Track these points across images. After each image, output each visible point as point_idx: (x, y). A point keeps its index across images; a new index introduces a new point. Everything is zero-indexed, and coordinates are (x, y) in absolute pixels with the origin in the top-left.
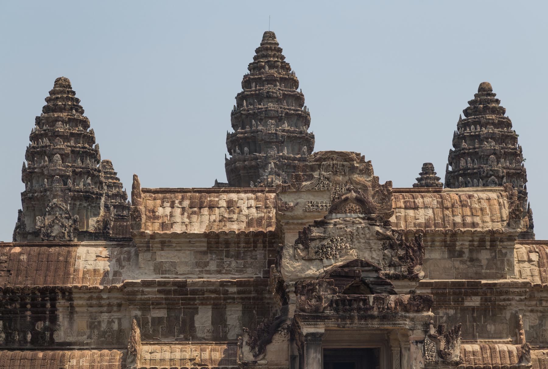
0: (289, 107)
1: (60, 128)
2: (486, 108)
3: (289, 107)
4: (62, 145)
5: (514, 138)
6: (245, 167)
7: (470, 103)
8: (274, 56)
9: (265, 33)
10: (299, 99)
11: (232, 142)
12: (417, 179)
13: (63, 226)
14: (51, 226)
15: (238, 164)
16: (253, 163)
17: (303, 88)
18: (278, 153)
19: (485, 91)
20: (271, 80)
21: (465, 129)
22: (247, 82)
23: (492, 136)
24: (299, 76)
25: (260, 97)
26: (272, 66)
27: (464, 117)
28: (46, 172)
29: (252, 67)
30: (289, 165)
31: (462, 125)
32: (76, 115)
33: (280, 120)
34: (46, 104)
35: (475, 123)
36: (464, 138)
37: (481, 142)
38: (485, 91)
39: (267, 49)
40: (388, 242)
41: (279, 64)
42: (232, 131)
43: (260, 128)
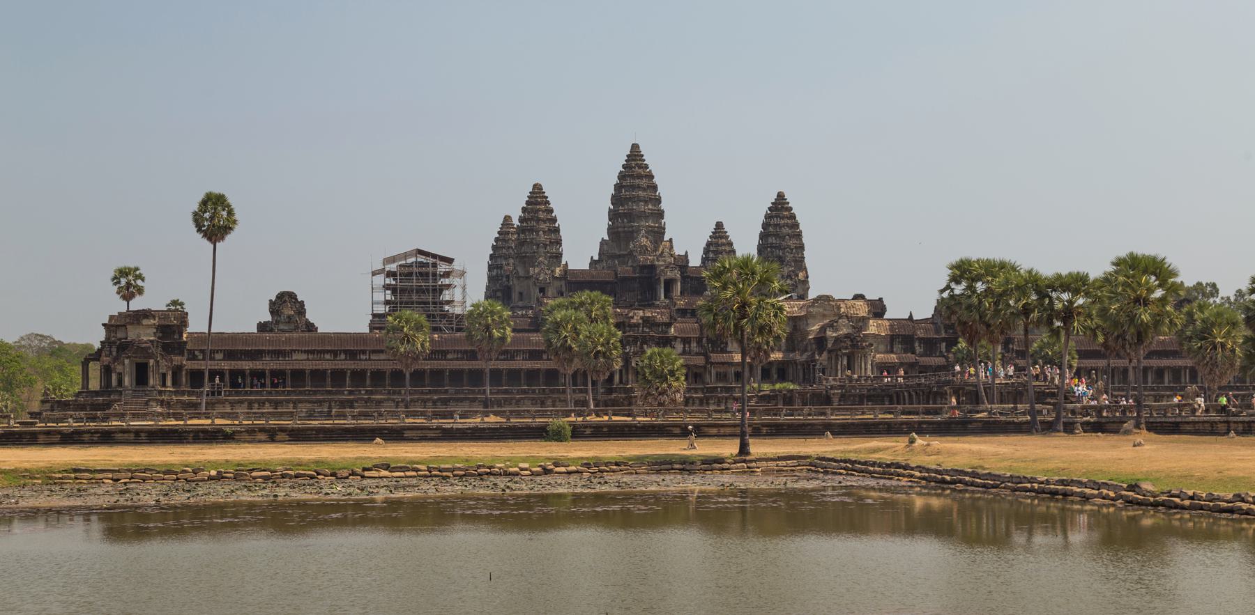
0: (650, 194)
1: (541, 215)
3: (650, 194)
4: (543, 226)
5: (797, 225)
10: (655, 188)
17: (657, 180)
19: (781, 196)
20: (640, 177)
22: (622, 176)
23: (787, 225)
25: (633, 187)
26: (640, 167)
31: (767, 216)
33: (646, 202)
35: (777, 217)
38: (781, 196)
40: (853, 327)
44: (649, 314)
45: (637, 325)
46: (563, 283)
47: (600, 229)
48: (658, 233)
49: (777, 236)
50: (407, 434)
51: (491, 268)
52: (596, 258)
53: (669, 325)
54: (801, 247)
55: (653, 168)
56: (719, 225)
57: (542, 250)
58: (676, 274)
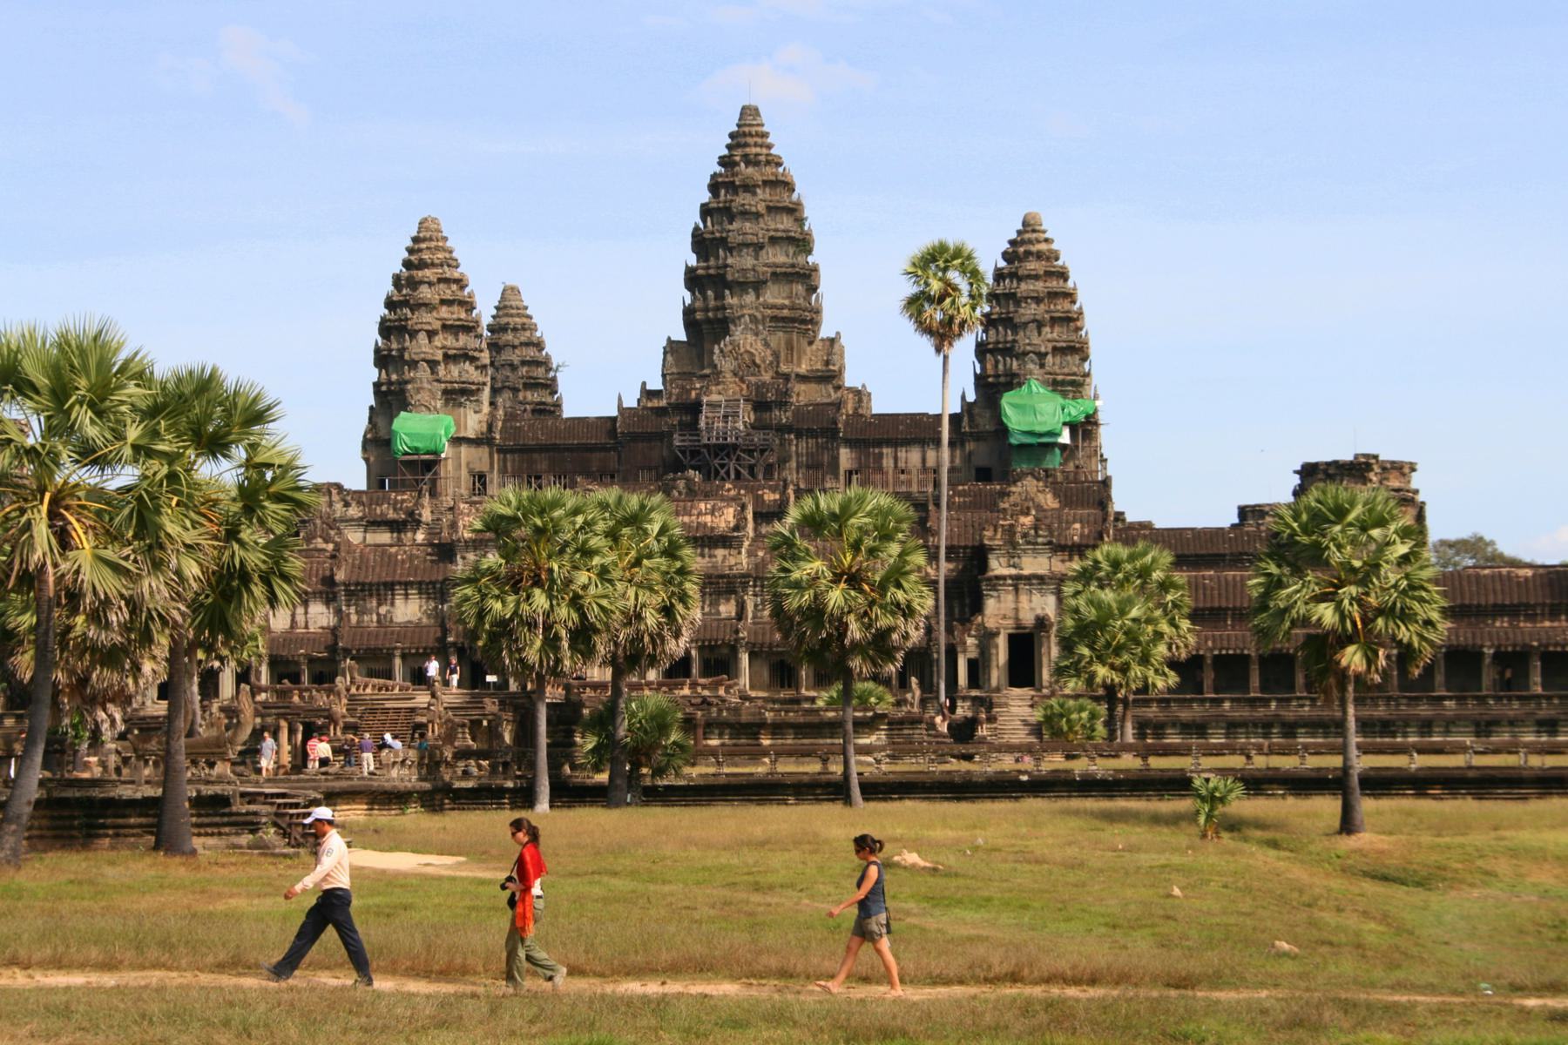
1: (425, 293)
2: (1028, 253)
6: (708, 321)
7: (1012, 243)
8: (756, 145)
9: (744, 108)
11: (693, 280)
16: (720, 315)
18: (758, 297)
20: (749, 188)
26: (750, 161)
27: (1002, 264)
28: (407, 357)
29: (724, 161)
30: (774, 319)
32: (448, 273)
34: (406, 254)
35: (1013, 275)
37: (1018, 303)
39: (744, 135)
41: (762, 158)
42: (692, 260)
43: (730, 261)
47: (664, 313)
48: (803, 321)
55: (794, 166)
57: (423, 372)
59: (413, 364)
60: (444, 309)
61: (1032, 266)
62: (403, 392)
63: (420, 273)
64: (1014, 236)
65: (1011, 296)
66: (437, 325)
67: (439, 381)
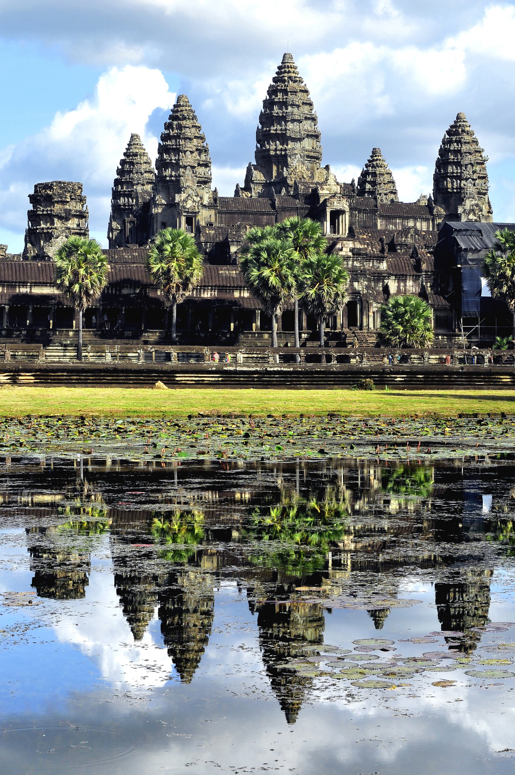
1: (188, 133)
4: (189, 145)
12: (369, 161)
13: (194, 201)
14: (185, 201)
15: (272, 153)
20: (295, 92)
21: (450, 146)
22: (272, 91)
24: (308, 88)
26: (295, 81)
30: (308, 156)
35: (459, 142)
36: (449, 151)
44: (358, 246)
45: (346, 258)
46: (212, 212)
48: (314, 157)
49: (458, 164)
50: (179, 378)
51: (116, 195)
52: (242, 185)
53: (380, 259)
54: (484, 178)
55: (309, 83)
56: (374, 152)
58: (344, 205)
59: (185, 167)
60: (195, 140)
61: (466, 138)
62: (178, 181)
63: (184, 122)
64: (453, 123)
65: (457, 152)
66: (194, 149)
67: (196, 176)
